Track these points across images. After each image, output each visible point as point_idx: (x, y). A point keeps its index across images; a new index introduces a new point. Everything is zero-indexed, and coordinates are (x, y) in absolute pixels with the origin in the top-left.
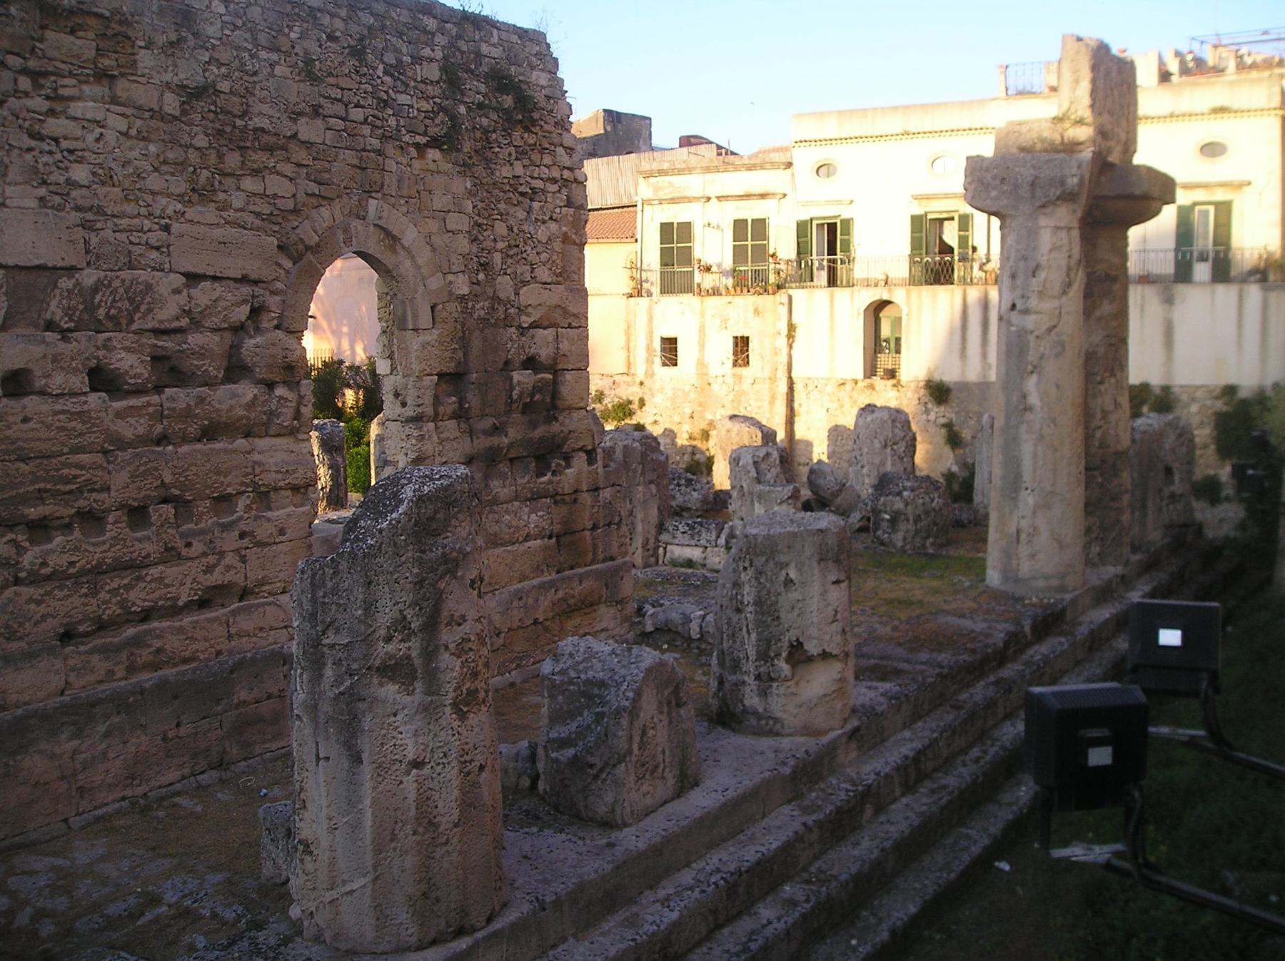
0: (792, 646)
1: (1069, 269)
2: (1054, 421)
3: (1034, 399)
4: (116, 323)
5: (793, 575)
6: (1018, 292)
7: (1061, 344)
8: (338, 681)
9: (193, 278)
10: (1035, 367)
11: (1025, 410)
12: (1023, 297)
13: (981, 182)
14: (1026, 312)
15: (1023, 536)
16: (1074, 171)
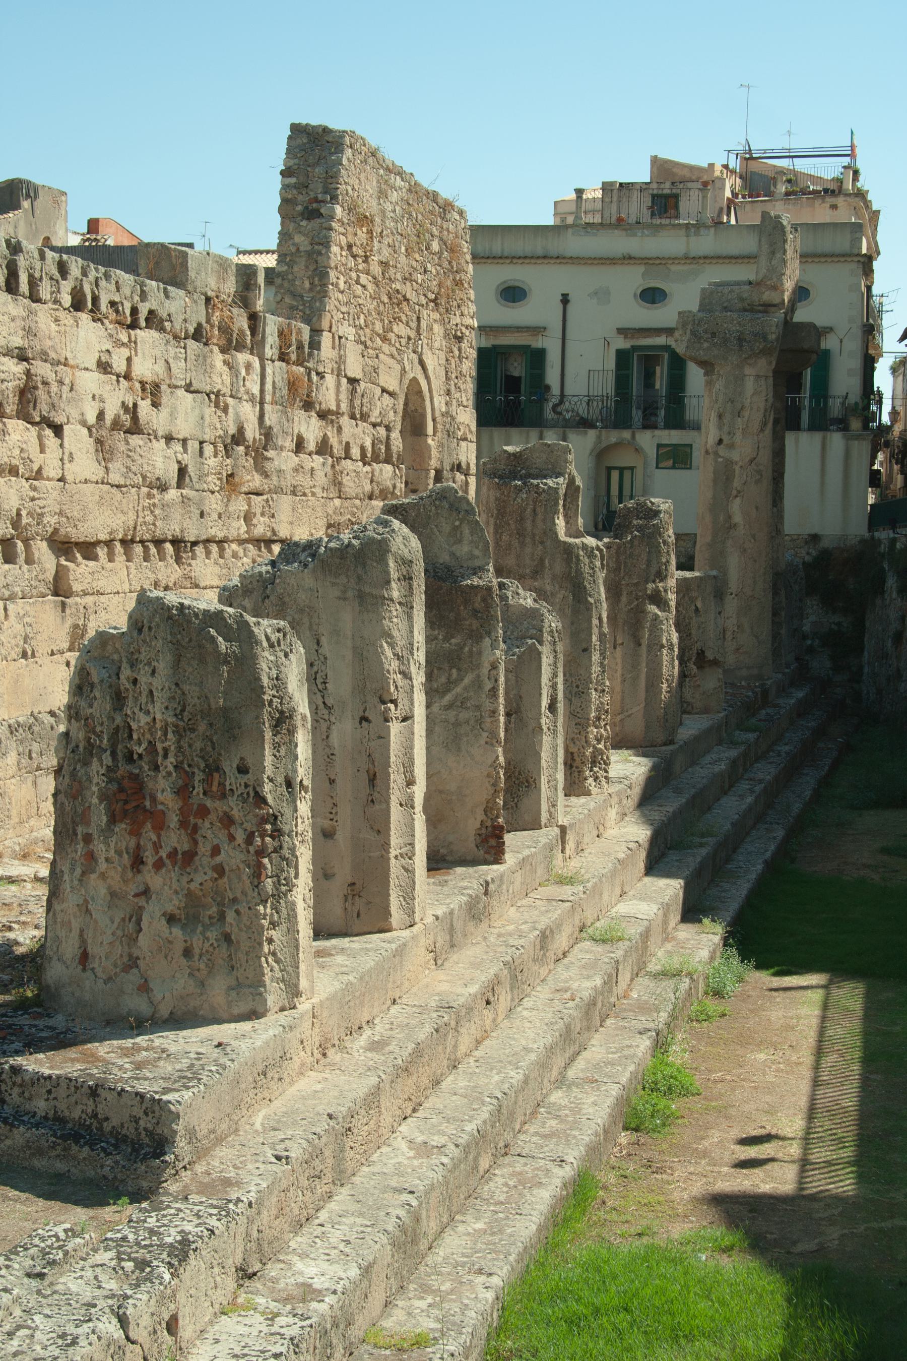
0: (698, 654)
1: (766, 410)
2: (754, 536)
3: (738, 518)
4: (364, 417)
5: (699, 605)
6: (726, 429)
7: (759, 472)
8: (630, 603)
9: (384, 390)
10: (739, 492)
11: (730, 528)
12: (729, 433)
13: (694, 333)
14: (731, 446)
15: (729, 635)
16: (774, 329)
